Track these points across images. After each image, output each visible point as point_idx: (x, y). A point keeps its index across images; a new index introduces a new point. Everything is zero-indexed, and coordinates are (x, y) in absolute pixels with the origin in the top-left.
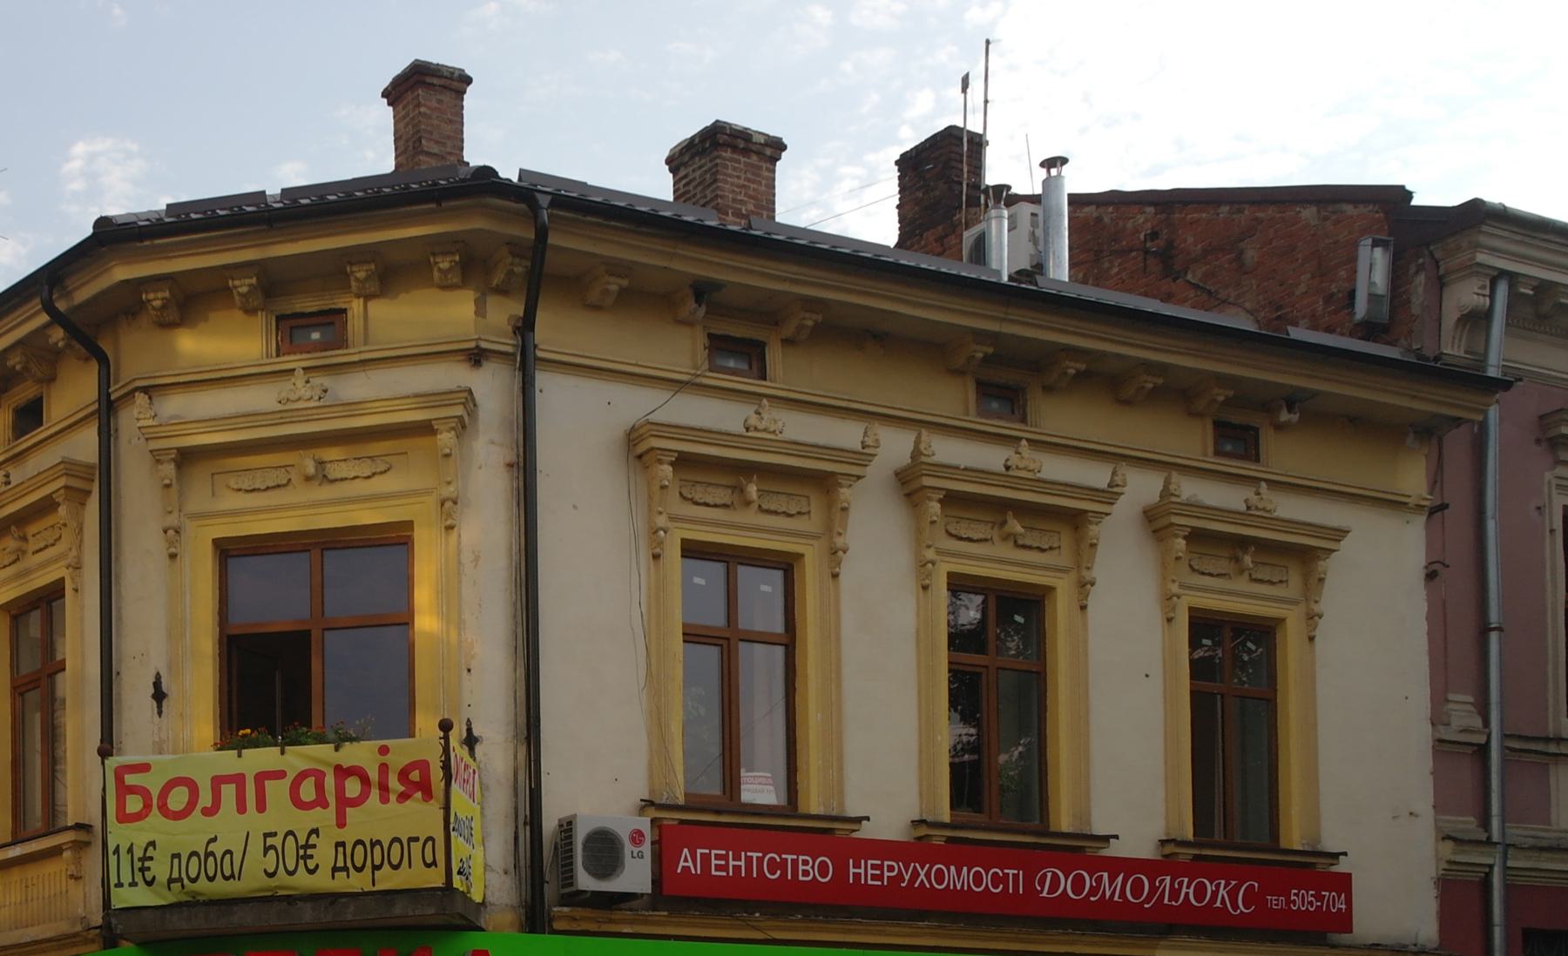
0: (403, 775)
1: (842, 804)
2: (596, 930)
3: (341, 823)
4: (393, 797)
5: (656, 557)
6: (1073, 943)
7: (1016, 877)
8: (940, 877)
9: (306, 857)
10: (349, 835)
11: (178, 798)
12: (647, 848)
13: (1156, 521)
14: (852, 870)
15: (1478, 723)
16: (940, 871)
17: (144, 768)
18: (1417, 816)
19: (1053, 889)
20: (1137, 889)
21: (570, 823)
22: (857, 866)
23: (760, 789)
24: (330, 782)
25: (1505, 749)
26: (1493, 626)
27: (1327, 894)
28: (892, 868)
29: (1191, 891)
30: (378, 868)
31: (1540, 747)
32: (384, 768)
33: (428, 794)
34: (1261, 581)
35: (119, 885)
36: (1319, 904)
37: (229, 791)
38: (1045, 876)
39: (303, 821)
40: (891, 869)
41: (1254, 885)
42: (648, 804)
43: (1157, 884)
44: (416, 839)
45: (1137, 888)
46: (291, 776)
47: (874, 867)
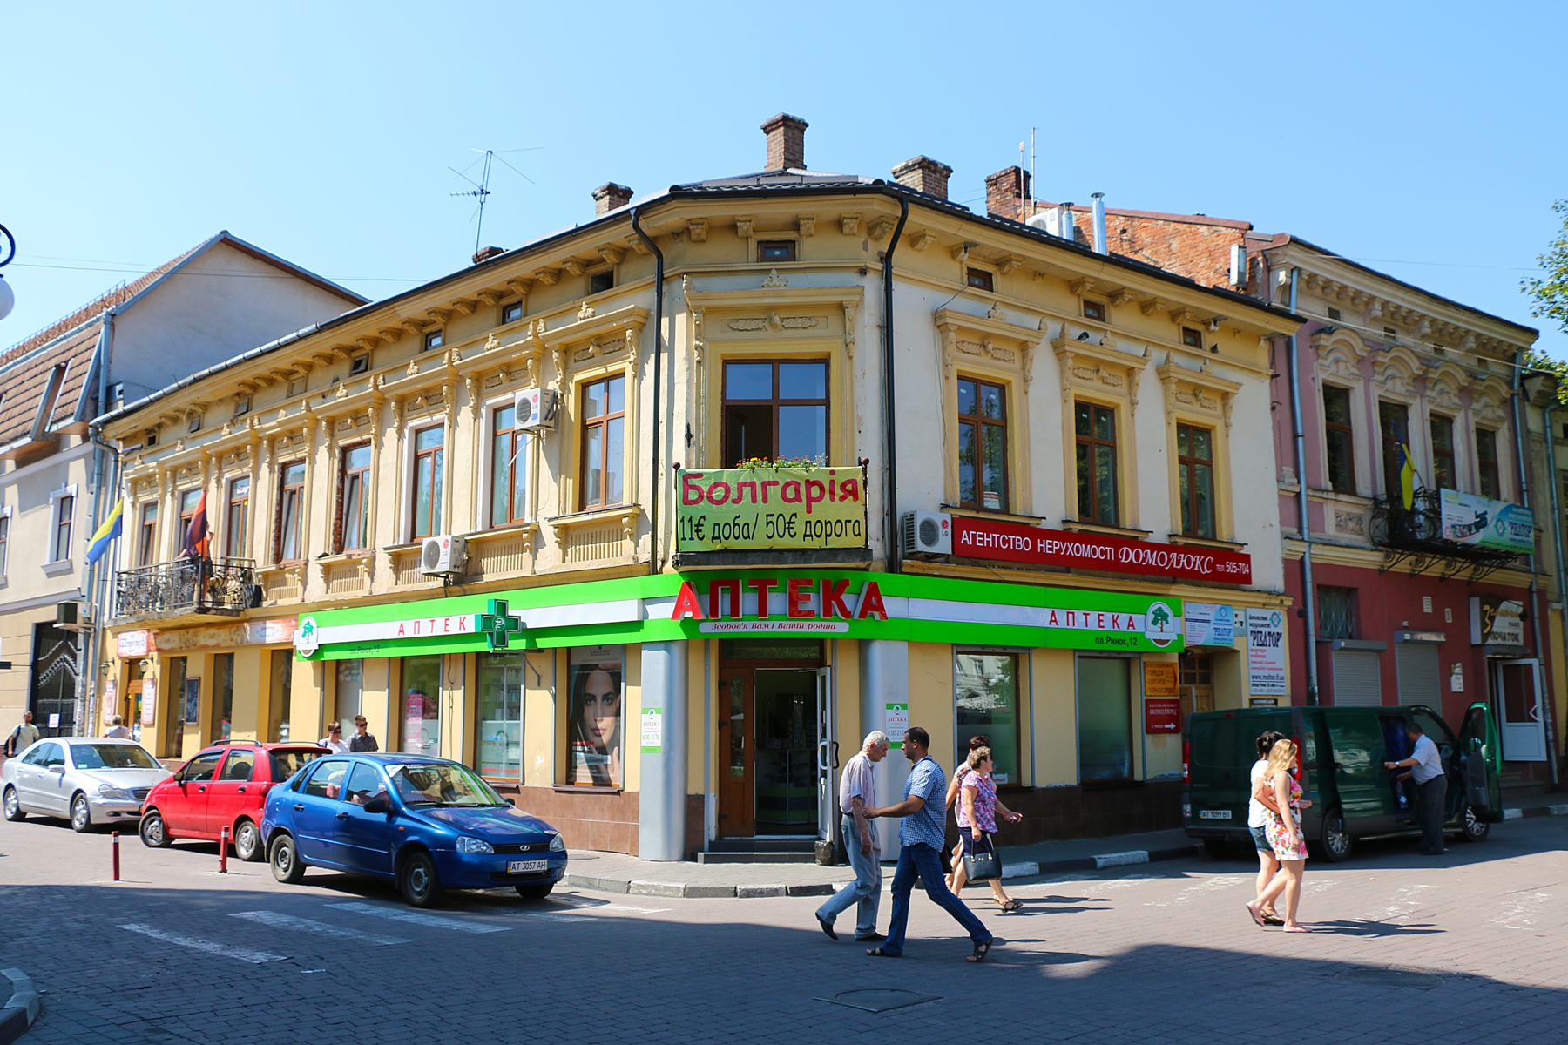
0: (843, 486)
1: (1031, 510)
3: (809, 511)
4: (837, 498)
5: (947, 378)
6: (1135, 586)
9: (789, 528)
10: (813, 518)
11: (719, 493)
12: (949, 530)
13: (1163, 374)
14: (1040, 545)
15: (1295, 481)
16: (1077, 547)
17: (699, 476)
19: (1127, 558)
21: (912, 515)
22: (1042, 543)
23: (992, 502)
24: (803, 490)
25: (1308, 495)
30: (830, 535)
32: (832, 482)
33: (856, 498)
34: (1205, 407)
35: (684, 539)
37: (747, 490)
39: (788, 509)
40: (1056, 545)
42: (945, 506)
44: (850, 521)
45: (1162, 558)
46: (782, 484)
47: (1049, 544)
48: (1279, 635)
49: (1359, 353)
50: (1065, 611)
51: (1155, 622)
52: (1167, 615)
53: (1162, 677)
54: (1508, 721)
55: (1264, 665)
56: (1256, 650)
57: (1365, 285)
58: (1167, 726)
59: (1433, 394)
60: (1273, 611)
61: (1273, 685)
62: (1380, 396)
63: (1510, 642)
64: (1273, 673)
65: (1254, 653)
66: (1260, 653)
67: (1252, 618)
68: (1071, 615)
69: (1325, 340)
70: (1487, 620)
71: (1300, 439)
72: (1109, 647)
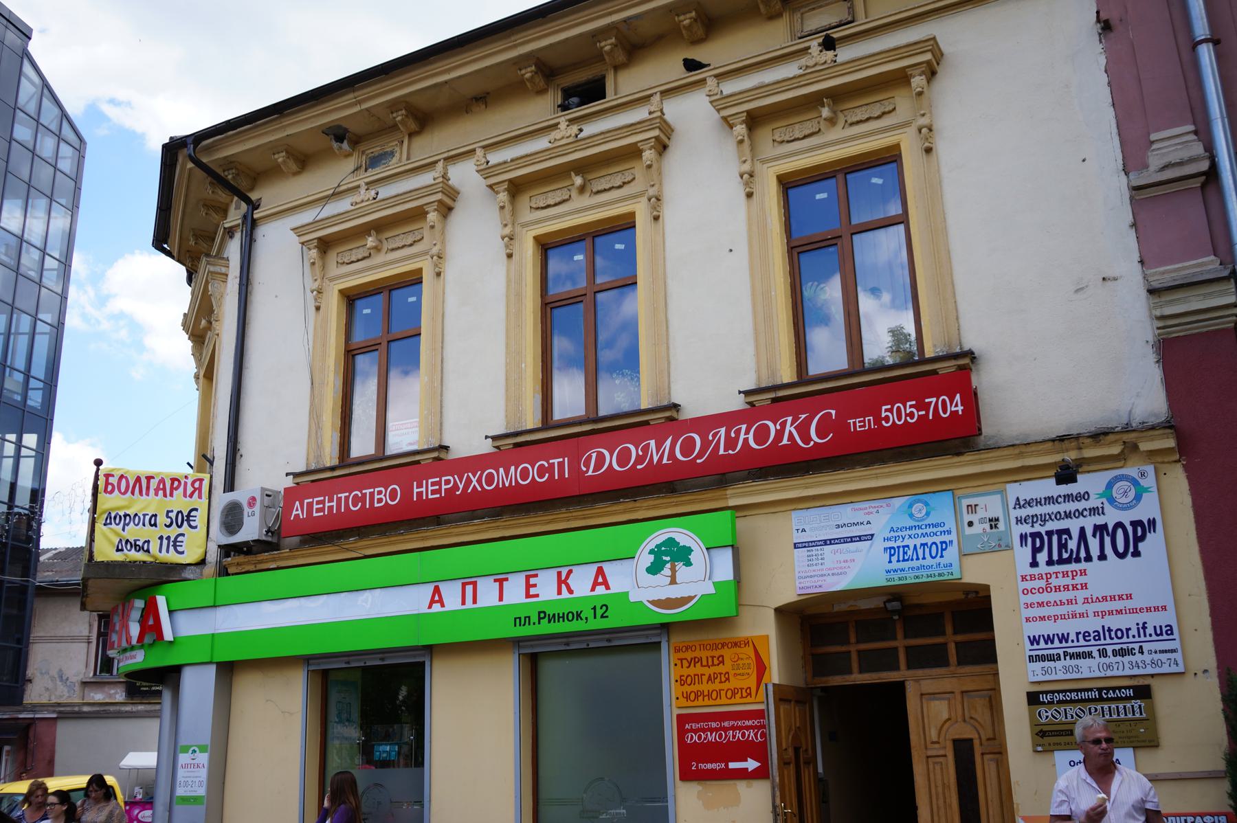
2: (254, 569)
7: (561, 465)
8: (490, 479)
12: (257, 508)
14: (416, 490)
15: (1198, 149)
18: (1115, 279)
20: (688, 447)
22: (419, 486)
26: (1198, 39)
27: (934, 400)
28: (448, 482)
29: (751, 436)
36: (923, 413)
38: (590, 457)
40: (447, 482)
41: (831, 413)
43: (710, 438)
47: (433, 484)
48: (1142, 529)
50: (458, 586)
51: (654, 569)
52: (689, 550)
53: (721, 669)
55: (1079, 608)
56: (1048, 576)
58: (732, 765)
60: (1105, 477)
61: (1122, 653)
64: (1115, 622)
65: (1042, 583)
66: (1062, 581)
67: (1018, 504)
68: (469, 589)
72: (546, 628)
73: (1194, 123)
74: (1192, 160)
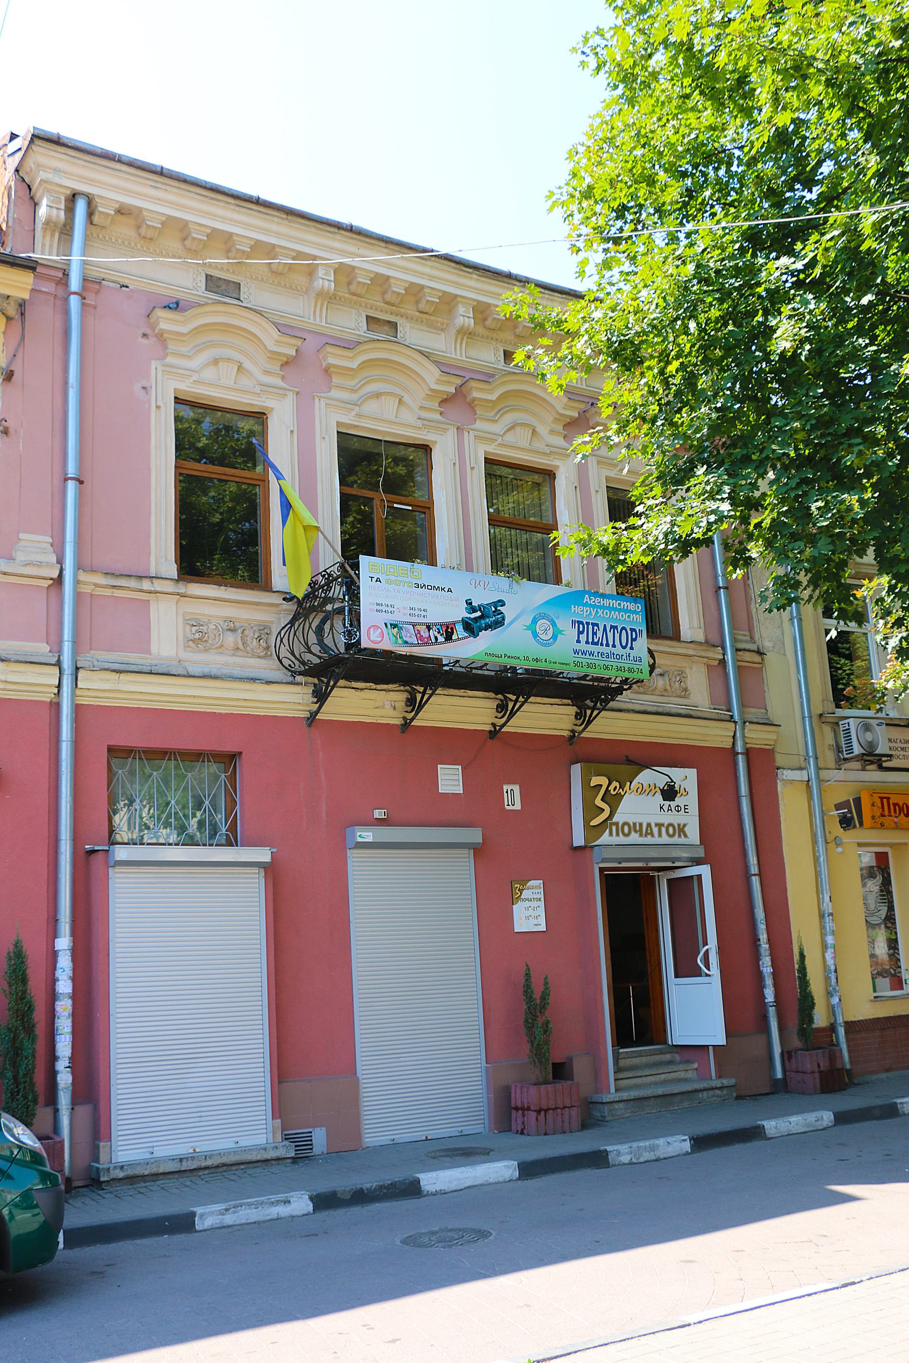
15: (53, 559)
25: (77, 582)
26: (70, 476)
31: (133, 583)
49: (272, 347)
54: (677, 976)
57: (278, 235)
59: (498, 428)
62: (339, 424)
63: (665, 839)
69: (166, 321)
70: (598, 802)
71: (71, 485)
73: (52, 537)
74: (48, 565)
